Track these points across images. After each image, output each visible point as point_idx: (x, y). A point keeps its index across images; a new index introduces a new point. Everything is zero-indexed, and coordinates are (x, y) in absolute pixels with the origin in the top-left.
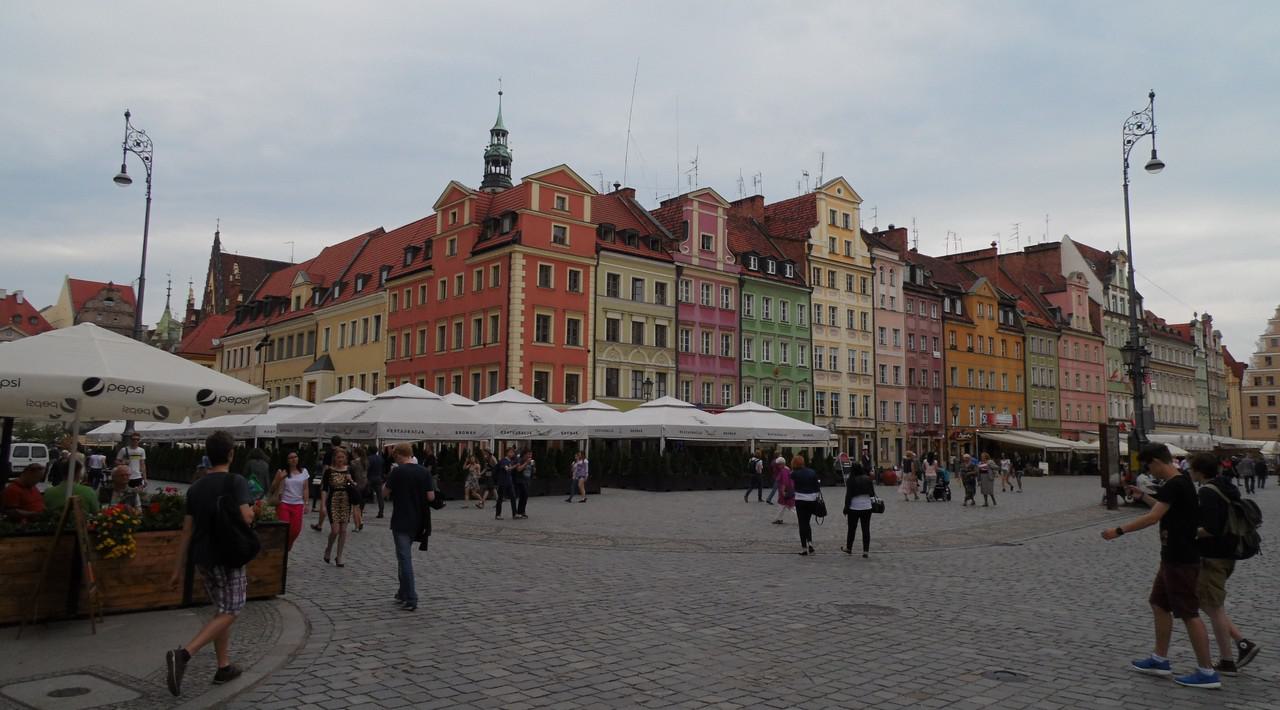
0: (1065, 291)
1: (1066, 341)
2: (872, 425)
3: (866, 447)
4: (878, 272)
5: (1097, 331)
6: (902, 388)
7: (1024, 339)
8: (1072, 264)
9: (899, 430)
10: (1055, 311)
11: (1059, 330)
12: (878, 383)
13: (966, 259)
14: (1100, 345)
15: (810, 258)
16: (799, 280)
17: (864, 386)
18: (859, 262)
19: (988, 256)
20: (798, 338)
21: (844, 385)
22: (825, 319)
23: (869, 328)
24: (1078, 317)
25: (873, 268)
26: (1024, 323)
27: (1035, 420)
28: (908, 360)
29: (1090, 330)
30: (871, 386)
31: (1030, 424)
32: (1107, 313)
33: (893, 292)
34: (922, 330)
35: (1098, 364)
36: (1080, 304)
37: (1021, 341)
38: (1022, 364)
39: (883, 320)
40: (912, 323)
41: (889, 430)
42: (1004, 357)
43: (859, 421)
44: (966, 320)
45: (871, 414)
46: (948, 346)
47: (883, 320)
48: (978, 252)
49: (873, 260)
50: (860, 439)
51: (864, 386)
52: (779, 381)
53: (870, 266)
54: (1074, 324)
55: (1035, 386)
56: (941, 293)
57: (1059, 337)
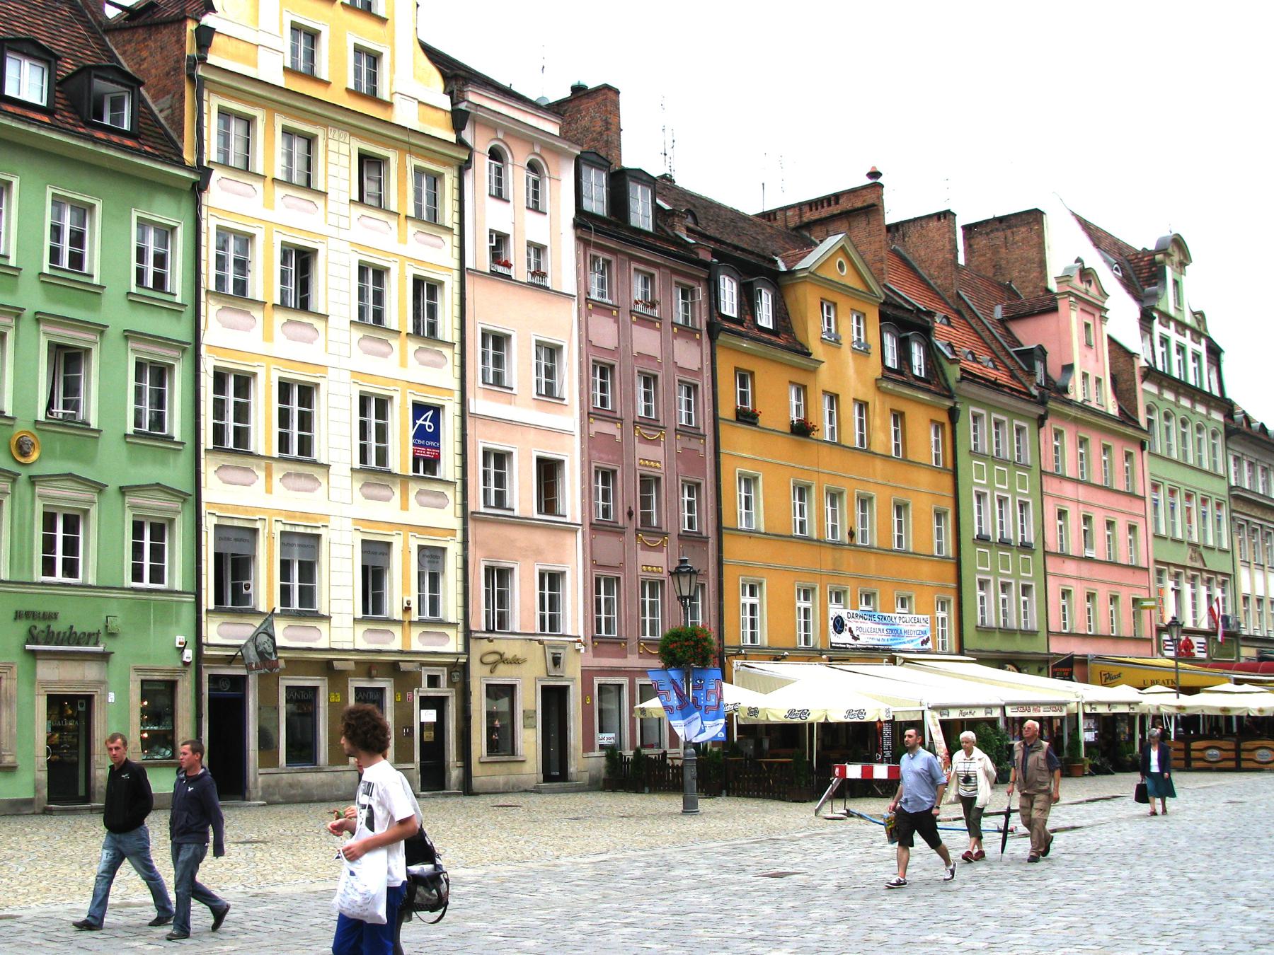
0: (1055, 310)
1: (1058, 434)
2: (452, 643)
3: (430, 716)
4: (482, 163)
5: (1127, 416)
6: (570, 529)
7: (953, 414)
8: (1064, 250)
9: (556, 661)
10: (1033, 356)
11: (1042, 402)
12: (477, 504)
13: (809, 216)
14: (1135, 451)
15: (200, 71)
16: (159, 138)
17: (420, 514)
18: (405, 115)
19: (858, 204)
20: (129, 335)
21: (340, 509)
22: (265, 277)
23: (447, 326)
24: (1085, 376)
25: (461, 143)
26: (953, 373)
27: (984, 630)
28: (592, 443)
29: (1113, 410)
30: (449, 517)
31: (971, 641)
32: (1151, 373)
33: (534, 228)
34: (641, 355)
35: (1132, 495)
36: (1089, 345)
37: (944, 418)
38: (947, 480)
39: (494, 307)
40: (605, 331)
41: (516, 661)
42: (902, 458)
43: (397, 630)
44: (786, 339)
45: (450, 608)
46: (727, 411)
47: (494, 307)
48: (837, 197)
49: (459, 119)
50: (398, 688)
51: (420, 514)
52: (33, 480)
53: (452, 137)
54: (1077, 392)
55: (982, 539)
56: (705, 256)
57: (1041, 421)
